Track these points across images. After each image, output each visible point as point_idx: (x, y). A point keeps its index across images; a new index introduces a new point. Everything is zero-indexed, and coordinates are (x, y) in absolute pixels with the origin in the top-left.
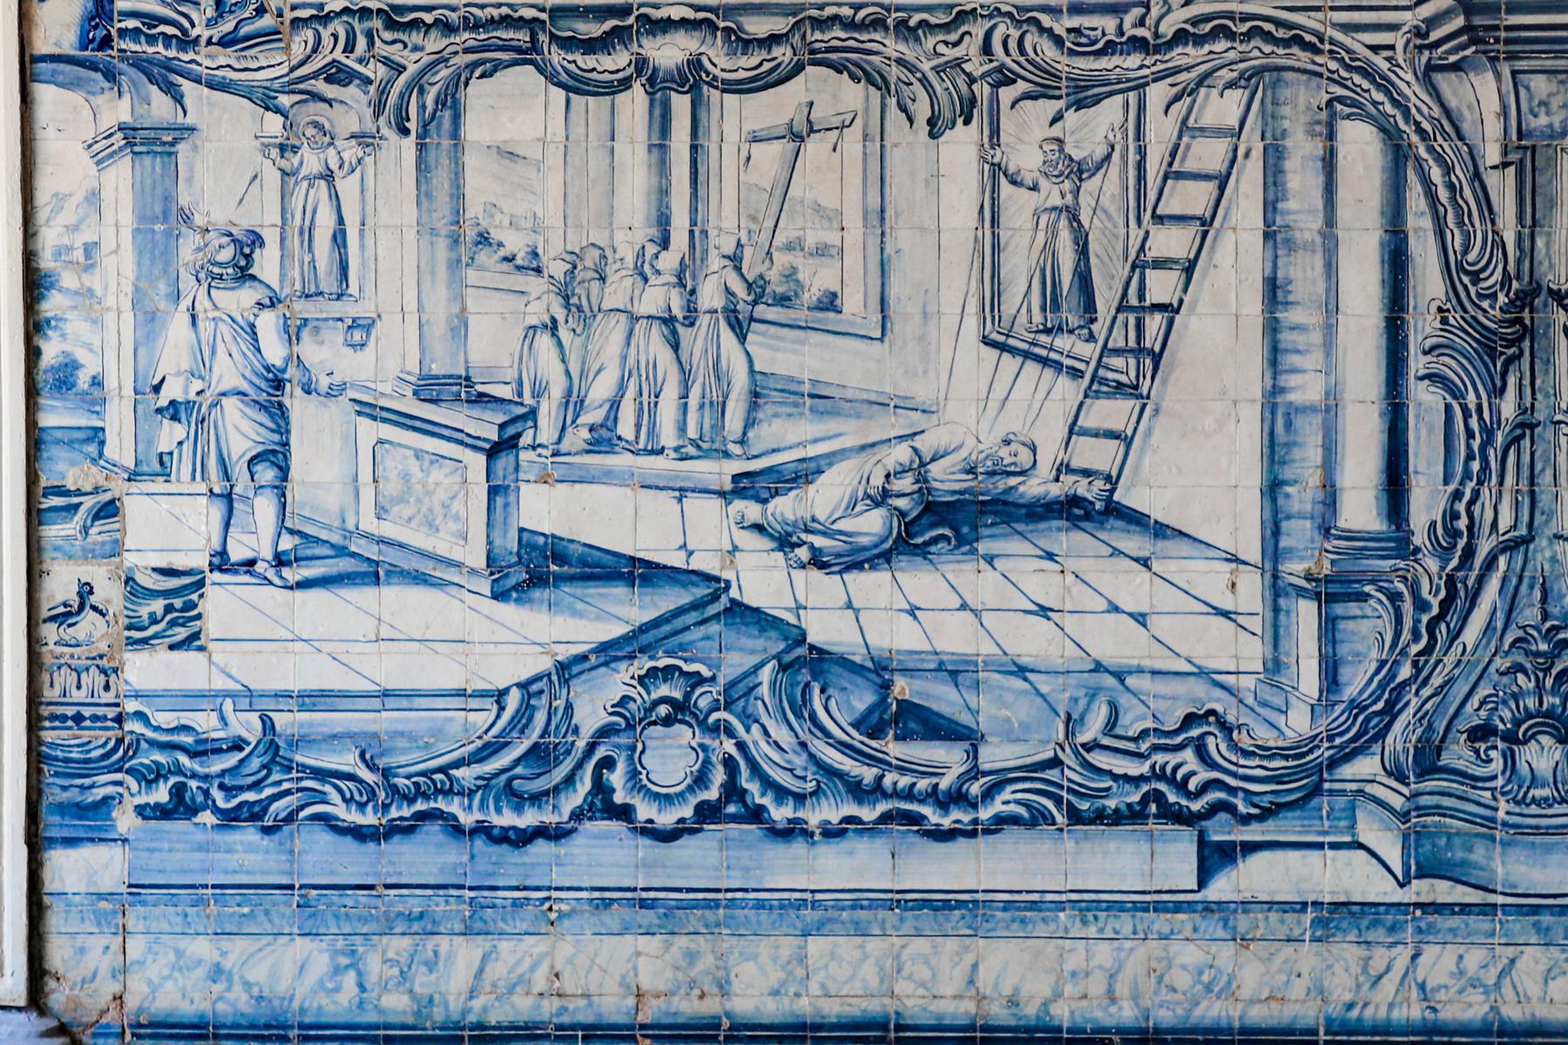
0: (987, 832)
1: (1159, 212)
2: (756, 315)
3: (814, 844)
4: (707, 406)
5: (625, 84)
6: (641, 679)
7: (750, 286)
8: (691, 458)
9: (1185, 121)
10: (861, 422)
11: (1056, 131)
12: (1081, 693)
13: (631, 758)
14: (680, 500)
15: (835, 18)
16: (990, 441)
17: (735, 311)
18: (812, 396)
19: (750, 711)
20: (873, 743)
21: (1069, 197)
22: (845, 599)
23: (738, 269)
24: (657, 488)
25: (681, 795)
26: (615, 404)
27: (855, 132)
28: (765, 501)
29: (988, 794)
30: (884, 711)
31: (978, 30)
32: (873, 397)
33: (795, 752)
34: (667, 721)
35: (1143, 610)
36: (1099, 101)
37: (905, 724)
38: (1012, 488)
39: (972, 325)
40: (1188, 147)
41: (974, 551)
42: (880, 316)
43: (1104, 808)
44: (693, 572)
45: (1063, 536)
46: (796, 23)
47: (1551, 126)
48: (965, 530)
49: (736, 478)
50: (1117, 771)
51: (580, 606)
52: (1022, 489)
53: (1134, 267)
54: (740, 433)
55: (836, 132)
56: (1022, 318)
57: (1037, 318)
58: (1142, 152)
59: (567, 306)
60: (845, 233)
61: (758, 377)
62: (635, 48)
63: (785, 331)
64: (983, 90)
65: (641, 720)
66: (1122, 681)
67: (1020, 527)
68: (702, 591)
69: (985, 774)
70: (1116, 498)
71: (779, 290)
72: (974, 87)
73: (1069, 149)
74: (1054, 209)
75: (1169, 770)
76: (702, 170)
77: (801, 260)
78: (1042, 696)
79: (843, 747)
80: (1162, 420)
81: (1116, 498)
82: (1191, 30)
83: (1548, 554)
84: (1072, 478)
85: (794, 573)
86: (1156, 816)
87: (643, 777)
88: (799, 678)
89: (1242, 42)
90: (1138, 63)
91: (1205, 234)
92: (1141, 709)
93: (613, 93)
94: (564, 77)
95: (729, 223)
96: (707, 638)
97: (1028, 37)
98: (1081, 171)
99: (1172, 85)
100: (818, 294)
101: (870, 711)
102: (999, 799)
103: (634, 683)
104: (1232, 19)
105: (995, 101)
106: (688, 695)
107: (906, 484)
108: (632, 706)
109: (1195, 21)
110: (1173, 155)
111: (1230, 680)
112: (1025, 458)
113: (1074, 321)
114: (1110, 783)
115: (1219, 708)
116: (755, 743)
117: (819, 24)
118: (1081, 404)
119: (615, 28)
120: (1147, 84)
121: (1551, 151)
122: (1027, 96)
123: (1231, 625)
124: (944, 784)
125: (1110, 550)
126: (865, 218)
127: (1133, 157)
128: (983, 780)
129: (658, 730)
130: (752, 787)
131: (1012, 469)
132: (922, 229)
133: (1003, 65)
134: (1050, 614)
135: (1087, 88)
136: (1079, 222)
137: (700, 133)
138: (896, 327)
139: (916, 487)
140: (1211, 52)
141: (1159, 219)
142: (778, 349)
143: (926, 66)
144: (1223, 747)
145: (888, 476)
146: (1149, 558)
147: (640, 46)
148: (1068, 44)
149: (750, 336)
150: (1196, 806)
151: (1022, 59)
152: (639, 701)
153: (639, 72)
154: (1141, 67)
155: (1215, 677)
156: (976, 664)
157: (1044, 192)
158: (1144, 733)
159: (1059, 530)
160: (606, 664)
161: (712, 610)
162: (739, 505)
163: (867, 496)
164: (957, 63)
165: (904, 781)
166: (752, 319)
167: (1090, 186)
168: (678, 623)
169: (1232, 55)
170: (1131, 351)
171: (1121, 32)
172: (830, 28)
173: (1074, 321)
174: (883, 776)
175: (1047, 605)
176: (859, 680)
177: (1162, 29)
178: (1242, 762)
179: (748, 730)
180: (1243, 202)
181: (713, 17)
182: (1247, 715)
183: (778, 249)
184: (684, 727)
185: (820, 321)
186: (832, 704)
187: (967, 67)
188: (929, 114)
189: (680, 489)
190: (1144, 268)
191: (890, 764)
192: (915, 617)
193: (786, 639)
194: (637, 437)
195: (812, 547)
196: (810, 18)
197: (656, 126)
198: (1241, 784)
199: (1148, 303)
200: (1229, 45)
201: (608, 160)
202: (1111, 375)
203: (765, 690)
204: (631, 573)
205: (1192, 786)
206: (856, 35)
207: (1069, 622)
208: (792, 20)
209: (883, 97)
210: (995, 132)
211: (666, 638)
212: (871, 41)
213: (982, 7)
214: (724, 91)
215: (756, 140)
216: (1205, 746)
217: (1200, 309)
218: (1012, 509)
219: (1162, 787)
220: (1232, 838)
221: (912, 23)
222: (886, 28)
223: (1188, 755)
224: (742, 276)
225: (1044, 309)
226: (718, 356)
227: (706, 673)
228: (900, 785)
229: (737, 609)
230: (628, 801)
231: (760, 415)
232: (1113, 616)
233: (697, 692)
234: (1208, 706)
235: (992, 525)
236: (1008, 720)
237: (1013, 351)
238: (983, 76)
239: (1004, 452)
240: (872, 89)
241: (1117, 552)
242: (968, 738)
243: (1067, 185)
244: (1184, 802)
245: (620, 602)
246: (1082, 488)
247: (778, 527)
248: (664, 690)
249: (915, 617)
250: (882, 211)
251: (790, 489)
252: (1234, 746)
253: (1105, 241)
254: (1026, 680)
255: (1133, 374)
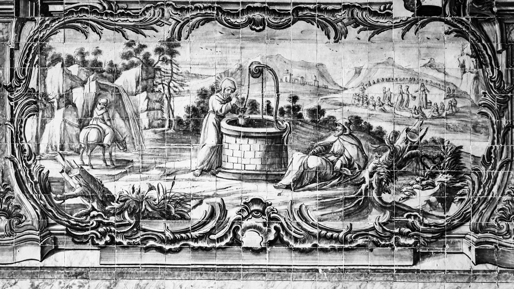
47: (3, 38)
83: (3, 163)
121: (4, 45)
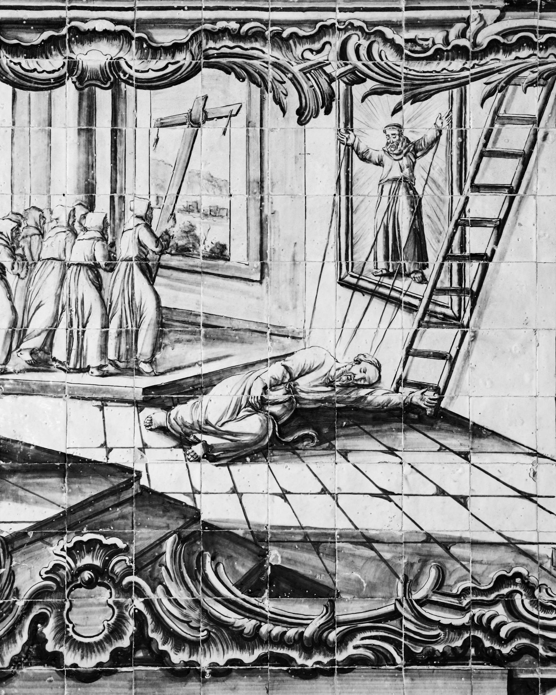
0: (342, 671)
1: (476, 182)
2: (163, 263)
3: (205, 682)
4: (124, 335)
5: (60, 82)
6: (70, 551)
7: (157, 240)
8: (112, 375)
9: (496, 112)
10: (245, 346)
11: (397, 119)
12: (416, 559)
13: (60, 616)
14: (102, 408)
15: (225, 31)
16: (345, 361)
17: (146, 259)
18: (206, 326)
19: (156, 574)
20: (253, 600)
21: (407, 171)
22: (232, 485)
23: (148, 227)
24: (84, 399)
25: (100, 643)
26: (51, 333)
27: (239, 122)
28: (168, 409)
29: (343, 640)
30: (261, 575)
31: (336, 40)
32: (254, 327)
33: (190, 607)
34: (90, 584)
35: (464, 494)
36: (431, 96)
37: (277, 585)
38: (362, 397)
39: (331, 269)
40: (499, 131)
41: (332, 447)
42: (259, 263)
43: (434, 651)
44: (112, 465)
45: (401, 435)
46: (194, 35)
48: (325, 430)
49: (146, 390)
50: (444, 621)
51: (21, 493)
52: (370, 398)
53: (456, 225)
54: (149, 355)
55: (225, 120)
56: (370, 265)
57: (382, 264)
58: (463, 135)
59: (13, 256)
60: (232, 198)
61: (164, 311)
62: (68, 53)
63: (185, 275)
64: (339, 87)
65: (69, 584)
66: (448, 550)
67: (368, 428)
68: (117, 481)
69: (341, 624)
70: (443, 405)
71: (181, 243)
72: (334, 85)
73: (406, 133)
74: (395, 180)
75: (484, 620)
76: (120, 149)
77: (198, 219)
78: (385, 561)
79: (228, 603)
80: (478, 343)
81: (443, 405)
82: (502, 40)
84: (408, 390)
85: (191, 465)
86: (474, 658)
87: (70, 630)
88: (195, 548)
89: (541, 50)
90: (460, 66)
91: (512, 200)
92: (465, 572)
93: (51, 89)
94: (11, 76)
95: (142, 191)
96: (123, 517)
97: (375, 46)
98: (416, 151)
99: (487, 84)
100: (211, 246)
101: (250, 574)
102: (351, 645)
103: (64, 554)
104: (534, 32)
105: (349, 96)
106: (106, 563)
107: (279, 394)
108: (62, 572)
109: (505, 34)
110: (487, 138)
111: (533, 549)
112: (372, 374)
113: (410, 266)
114: (438, 631)
115: (524, 571)
116: (160, 601)
117: (213, 35)
118: (416, 332)
119: (51, 37)
120: (467, 83)
122: (374, 92)
123: (535, 505)
124: (308, 632)
125: (439, 446)
126: (248, 187)
127: (456, 140)
128: (338, 630)
129: (83, 591)
130: (157, 637)
131: (362, 382)
132: (292, 196)
133: (355, 68)
134: (392, 497)
135: (421, 86)
136: (415, 192)
137: (119, 121)
138: (272, 273)
139: (287, 396)
140: (517, 58)
141: (476, 188)
142: (179, 289)
143: (296, 69)
144: (527, 602)
145: (265, 388)
146: (468, 453)
147: (72, 52)
148: (406, 51)
149: (158, 279)
150: (506, 650)
151: (370, 63)
152: (67, 568)
153: (71, 72)
154: (462, 70)
155: (521, 546)
156: (333, 536)
157: (387, 168)
158: (466, 591)
159: (399, 430)
160: (41, 539)
161: (126, 495)
162: (148, 411)
163: (249, 404)
164: (320, 66)
165: (277, 630)
166: (159, 266)
167: (423, 162)
168: (100, 505)
169: (533, 60)
170: (454, 291)
171: (446, 41)
172: (221, 39)
173: (410, 266)
174: (260, 626)
175: (389, 490)
176: (241, 549)
177: (479, 40)
178: (542, 614)
179: (154, 591)
180: (541, 174)
181: (128, 29)
182: (545, 576)
183: (180, 211)
184: (103, 589)
185: (215, 266)
186: (221, 569)
187: (328, 69)
188: (298, 106)
189: (102, 400)
190: (464, 226)
191: (265, 617)
192: (286, 500)
193: (185, 517)
194: (69, 358)
195: (205, 445)
196: (205, 30)
197: (85, 112)
198: (541, 633)
199: (467, 253)
200: (531, 52)
201: (46, 141)
202: (438, 309)
203: (167, 558)
204: (62, 466)
205: (503, 633)
206: (242, 44)
207: (406, 503)
208: (191, 32)
209: (262, 93)
210: (349, 120)
211: (90, 517)
212: (253, 49)
213: (339, 22)
214: (138, 87)
215: (163, 125)
216: (513, 602)
217: (507, 258)
218: (361, 414)
219: (480, 635)
220: (535, 676)
221: (285, 35)
222: (265, 39)
223: (500, 609)
224: (152, 232)
225: (386, 258)
226: (133, 295)
227: (121, 545)
228: (274, 633)
229: (146, 494)
230: (57, 649)
231: (166, 341)
232: (441, 498)
233: (114, 561)
234: (515, 570)
235: (346, 426)
236: (359, 582)
237: (363, 291)
238: (340, 77)
239: (356, 369)
240: (253, 86)
241: (443, 448)
242: (327, 596)
243: (405, 162)
244: (497, 647)
245: (53, 489)
246: (416, 397)
247: (179, 429)
248: (87, 560)
249: (286, 500)
250: (262, 181)
251: (189, 399)
252: (535, 602)
253: (434, 205)
254: (373, 549)
255: (456, 309)
